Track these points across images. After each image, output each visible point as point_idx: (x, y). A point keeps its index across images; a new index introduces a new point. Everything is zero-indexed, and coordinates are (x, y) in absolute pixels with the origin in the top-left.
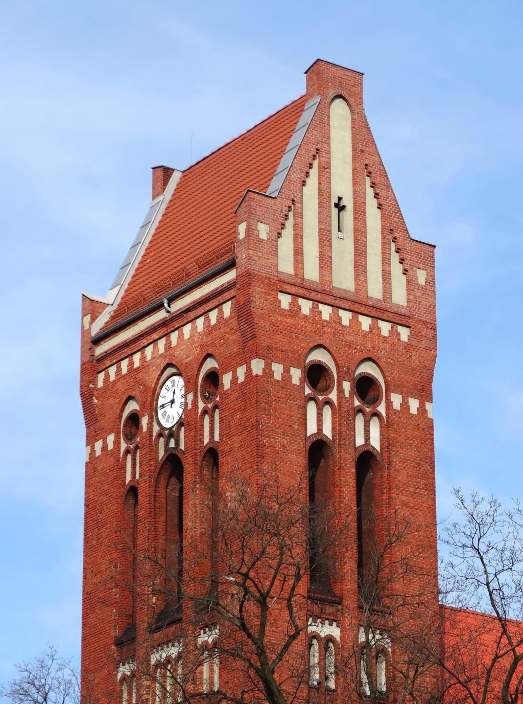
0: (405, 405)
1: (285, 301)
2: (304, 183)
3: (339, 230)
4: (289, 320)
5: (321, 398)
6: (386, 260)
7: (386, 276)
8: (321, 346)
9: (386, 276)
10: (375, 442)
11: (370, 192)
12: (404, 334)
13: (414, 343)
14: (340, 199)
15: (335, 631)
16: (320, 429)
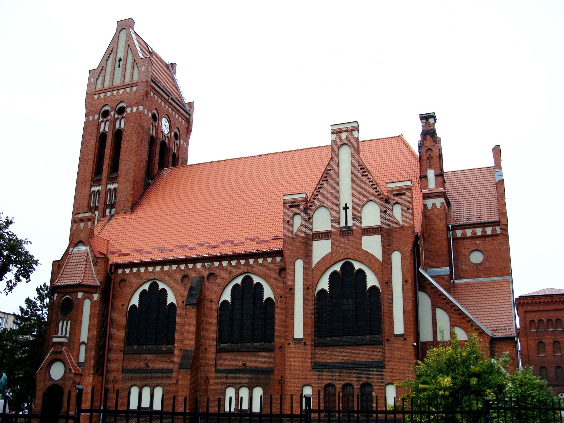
0: (132, 110)
1: (96, 97)
2: (107, 60)
3: (119, 67)
4: (97, 102)
5: (105, 120)
6: (133, 68)
7: (132, 73)
8: (106, 105)
9: (132, 73)
10: (122, 126)
11: (130, 51)
12: (134, 89)
13: (138, 89)
14: (120, 58)
15: (99, 188)
16: (104, 129)
